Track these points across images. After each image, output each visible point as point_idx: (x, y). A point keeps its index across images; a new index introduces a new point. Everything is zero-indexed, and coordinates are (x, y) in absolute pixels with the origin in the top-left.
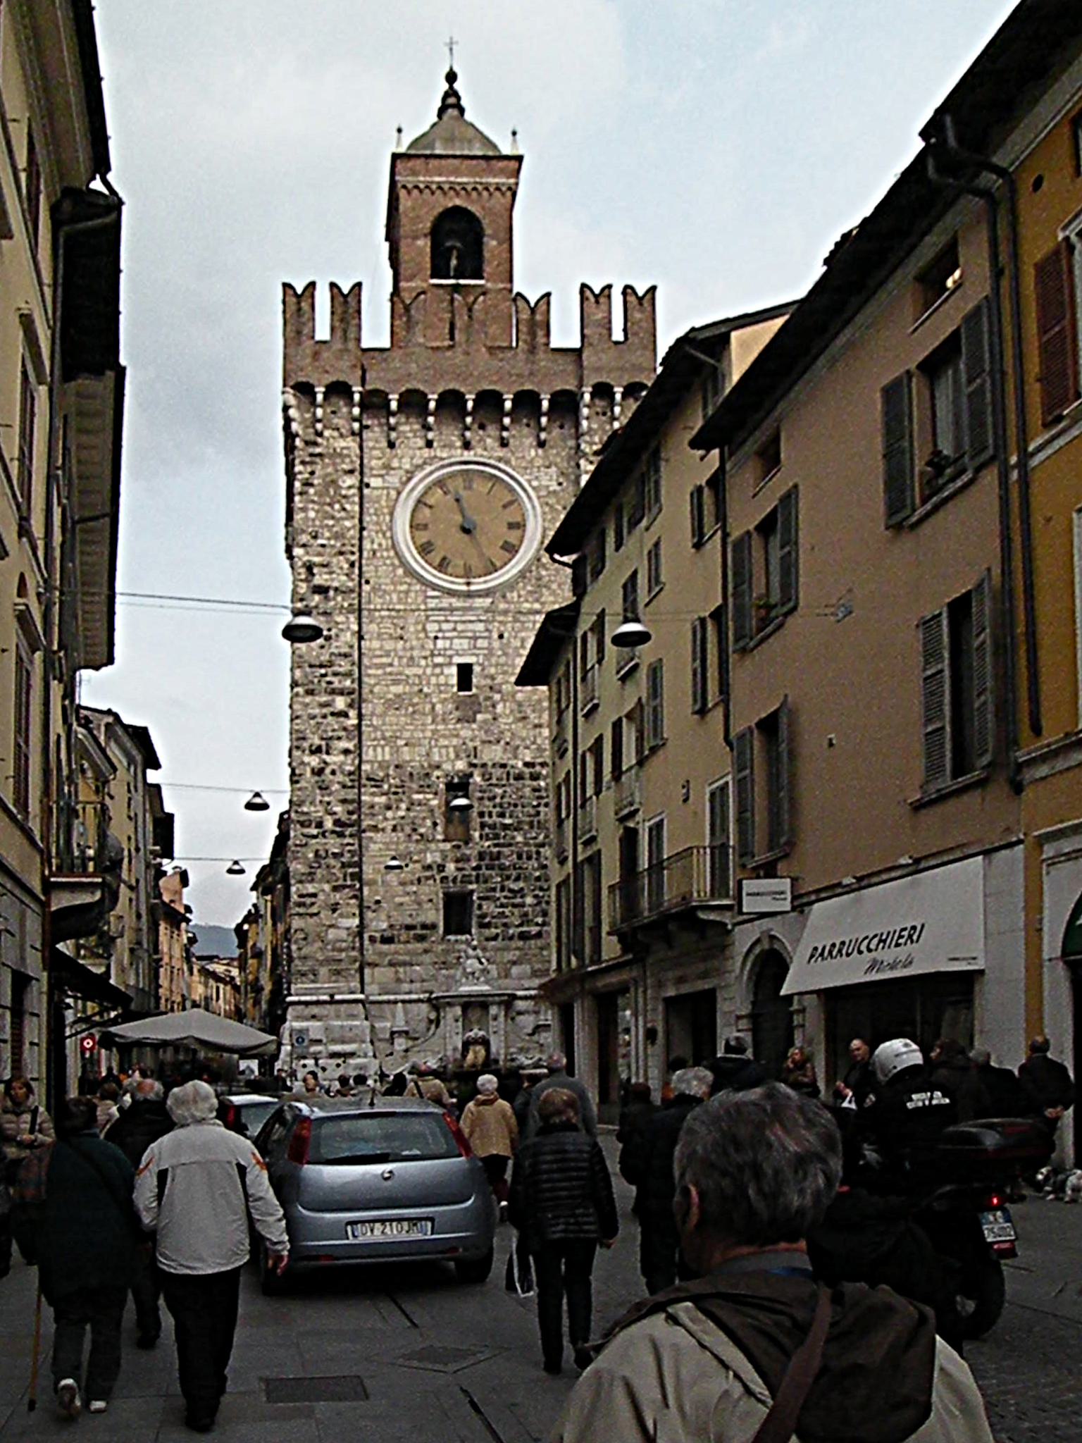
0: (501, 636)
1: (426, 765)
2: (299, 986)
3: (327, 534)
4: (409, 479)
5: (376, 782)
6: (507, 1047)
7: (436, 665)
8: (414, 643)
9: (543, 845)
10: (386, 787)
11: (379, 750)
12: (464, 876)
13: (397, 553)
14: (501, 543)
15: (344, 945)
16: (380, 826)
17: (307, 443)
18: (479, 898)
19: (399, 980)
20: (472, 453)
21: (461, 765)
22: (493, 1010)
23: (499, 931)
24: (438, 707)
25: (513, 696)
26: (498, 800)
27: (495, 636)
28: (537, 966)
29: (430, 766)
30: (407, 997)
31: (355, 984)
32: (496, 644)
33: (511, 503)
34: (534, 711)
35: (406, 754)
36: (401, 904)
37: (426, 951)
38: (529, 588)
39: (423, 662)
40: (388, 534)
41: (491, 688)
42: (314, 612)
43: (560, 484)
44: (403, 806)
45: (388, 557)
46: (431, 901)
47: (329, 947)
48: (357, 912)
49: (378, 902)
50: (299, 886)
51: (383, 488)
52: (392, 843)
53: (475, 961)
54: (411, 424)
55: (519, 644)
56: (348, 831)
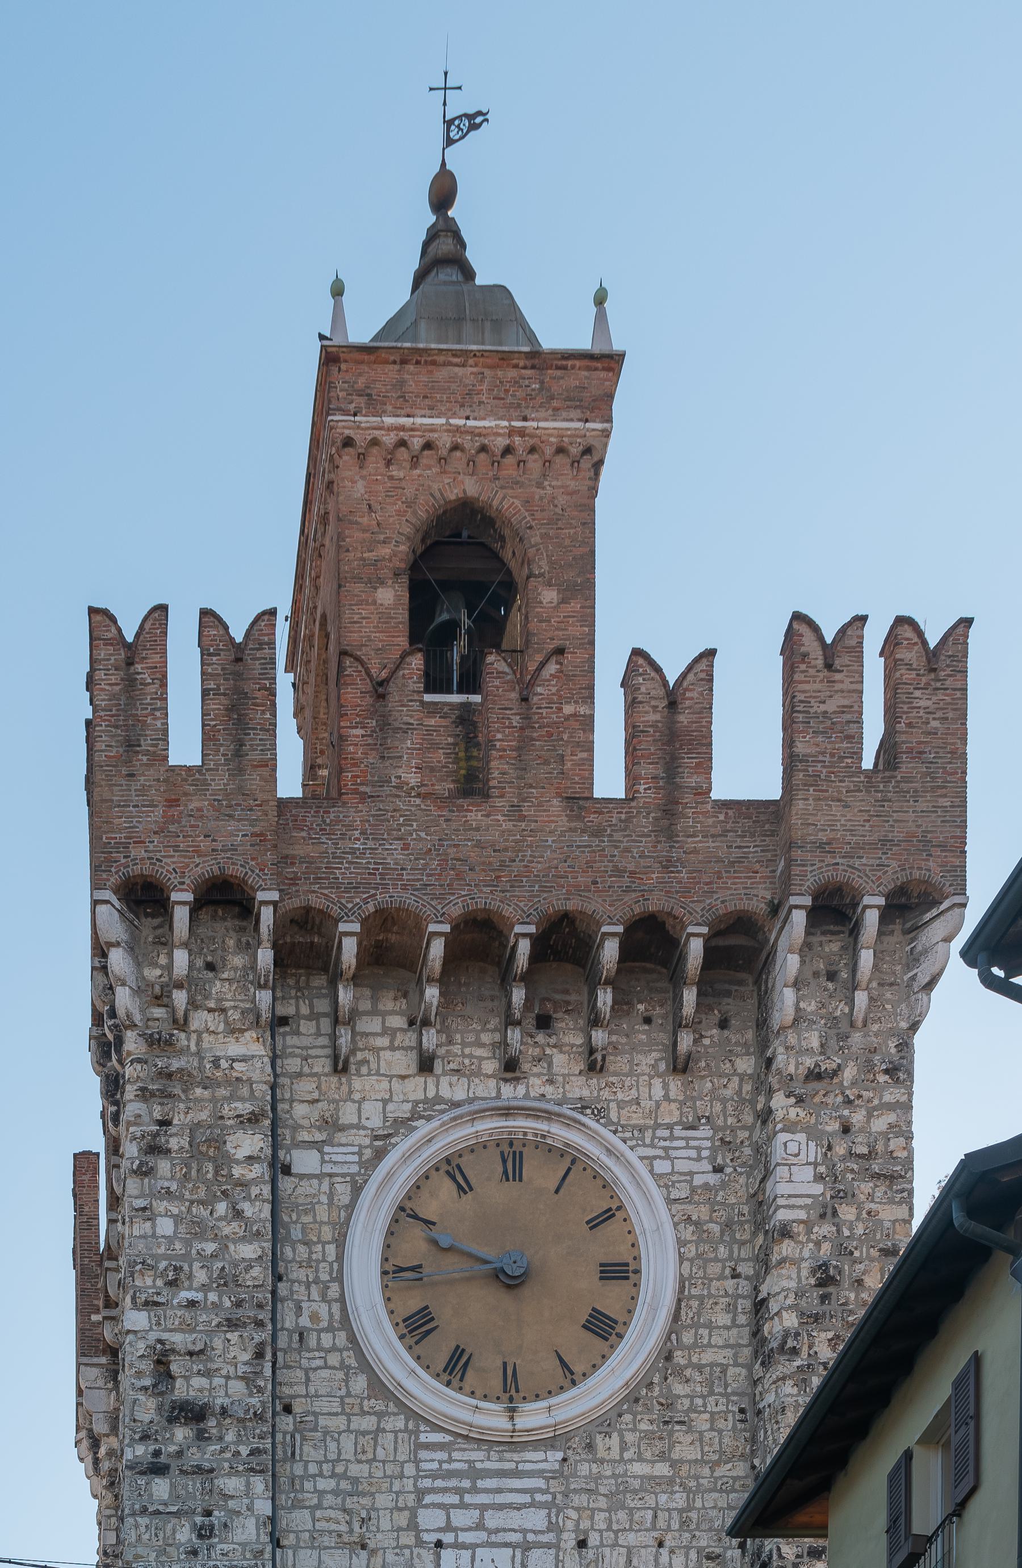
4: (380, 1155)
20: (521, 1090)
40: (334, 1291)
43: (718, 1170)
45: (334, 1349)
51: (320, 1177)
54: (384, 1014)
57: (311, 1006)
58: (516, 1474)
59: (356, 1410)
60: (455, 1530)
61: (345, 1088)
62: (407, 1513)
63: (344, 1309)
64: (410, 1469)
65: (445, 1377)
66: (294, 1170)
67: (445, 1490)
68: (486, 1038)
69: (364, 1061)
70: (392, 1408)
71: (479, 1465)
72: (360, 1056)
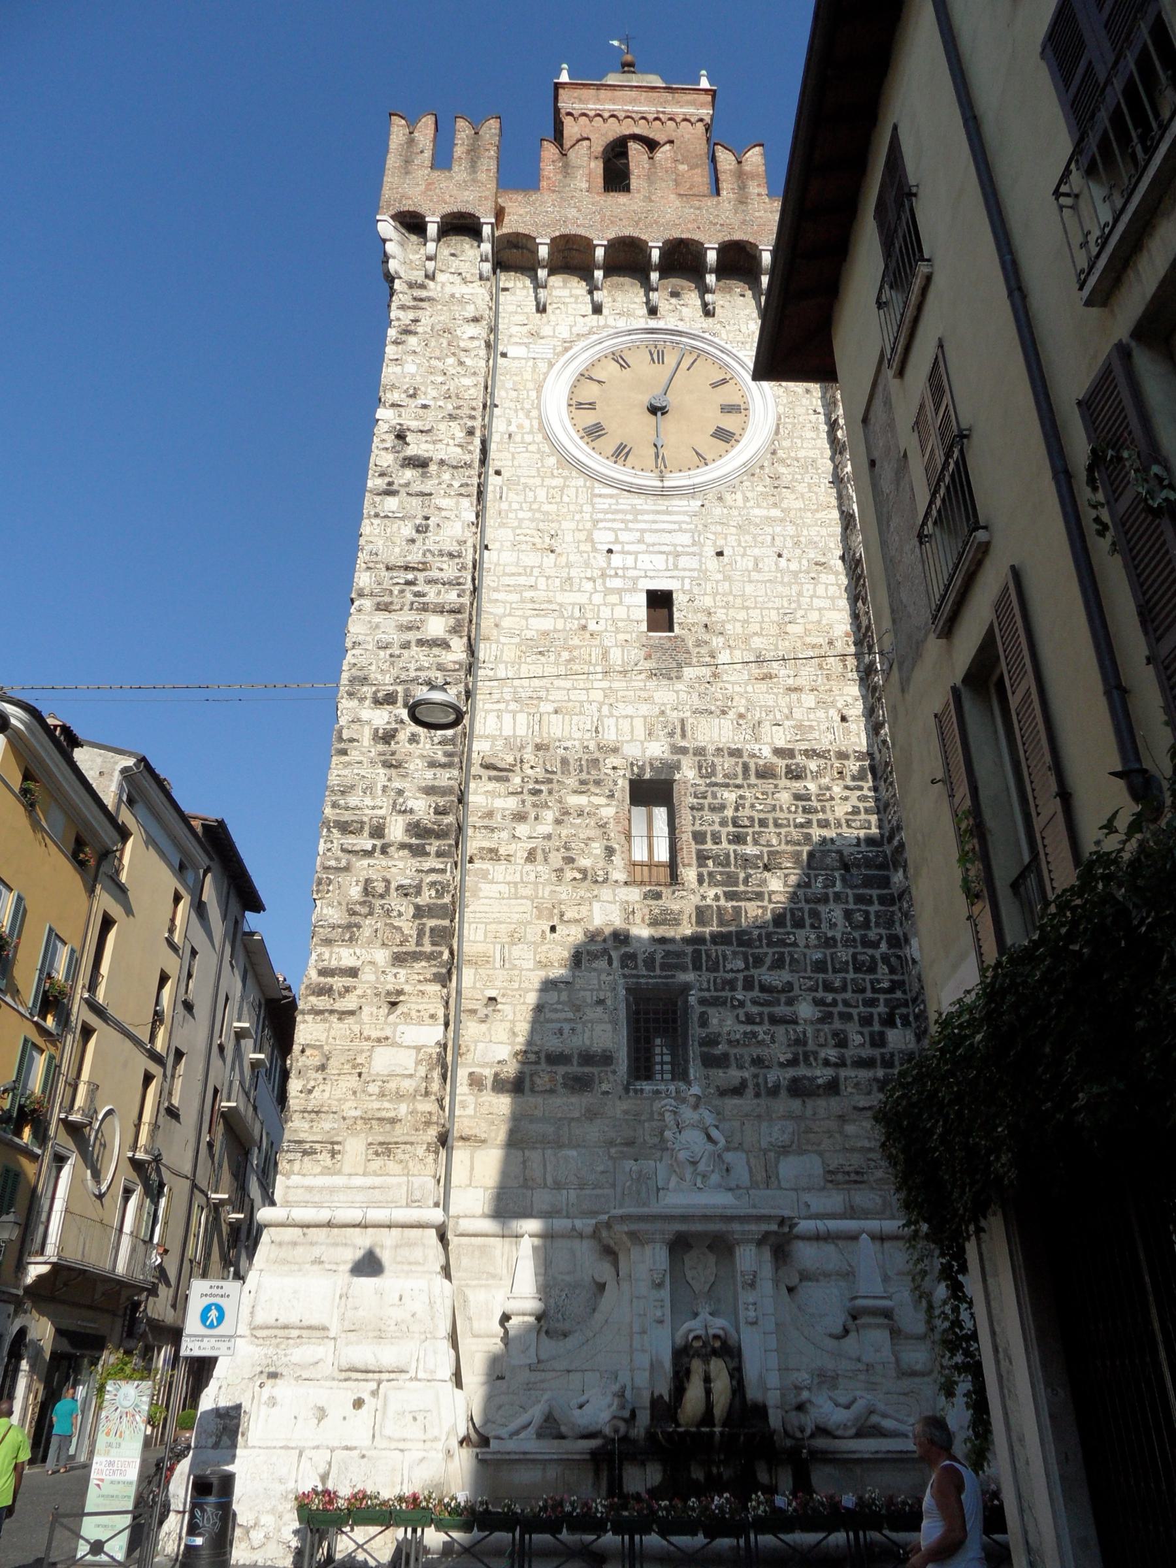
1: (592, 745)
3: (434, 393)
4: (566, 350)
6: (784, 1370)
7: (608, 591)
8: (572, 558)
9: (825, 899)
12: (668, 954)
13: (547, 438)
14: (712, 431)
15: (408, 1085)
17: (411, 285)
18: (702, 1002)
21: (658, 749)
22: (748, 1258)
24: (616, 656)
25: (746, 641)
26: (729, 813)
27: (710, 551)
28: (835, 1162)
29: (600, 748)
31: (425, 1183)
32: (712, 563)
38: (760, 489)
39: (588, 586)
41: (706, 626)
42: (403, 491)
46: (601, 1002)
48: (441, 1013)
50: (325, 951)
51: (528, 359)
52: (526, 884)
53: (700, 1137)
55: (751, 565)
56: (433, 846)
58: (667, 513)
59: (549, 474)
62: (585, 533)
63: (541, 423)
64: (587, 508)
65: (614, 459)
67: (614, 520)
68: (637, 300)
70: (574, 474)
71: (639, 507)
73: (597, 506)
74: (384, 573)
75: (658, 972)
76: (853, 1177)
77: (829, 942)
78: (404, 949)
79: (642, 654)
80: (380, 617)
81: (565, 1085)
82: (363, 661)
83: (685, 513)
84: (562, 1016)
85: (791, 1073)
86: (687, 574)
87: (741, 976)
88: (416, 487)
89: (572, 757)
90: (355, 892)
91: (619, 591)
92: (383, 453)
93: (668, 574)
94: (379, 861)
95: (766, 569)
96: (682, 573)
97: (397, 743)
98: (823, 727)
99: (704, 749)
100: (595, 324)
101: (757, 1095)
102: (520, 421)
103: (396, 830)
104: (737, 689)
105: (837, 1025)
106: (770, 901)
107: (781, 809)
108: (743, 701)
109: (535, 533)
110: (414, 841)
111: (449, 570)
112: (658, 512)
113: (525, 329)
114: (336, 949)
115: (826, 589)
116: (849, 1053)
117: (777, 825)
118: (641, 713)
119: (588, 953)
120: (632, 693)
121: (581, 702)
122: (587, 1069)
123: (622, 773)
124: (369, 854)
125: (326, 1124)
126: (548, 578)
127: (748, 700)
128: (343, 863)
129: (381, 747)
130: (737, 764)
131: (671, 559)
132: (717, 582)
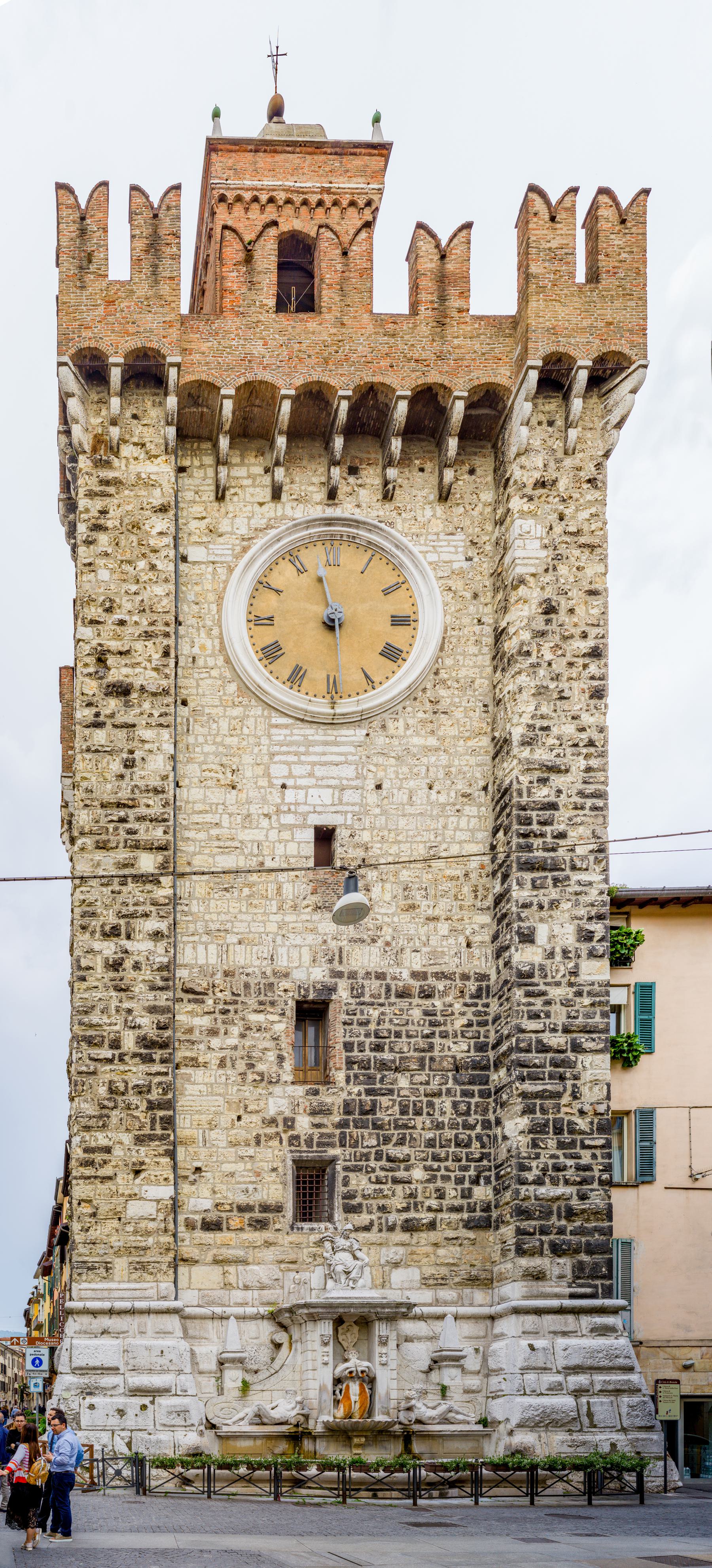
0: (379, 787)
1: (269, 972)
2: (85, 1285)
4: (245, 550)
5: (194, 994)
7: (282, 827)
9: (438, 1094)
10: (210, 1002)
11: (201, 948)
12: (322, 1135)
13: (228, 661)
14: (380, 648)
16: (201, 1060)
18: (346, 1169)
19: (227, 1286)
21: (319, 974)
23: (374, 1217)
26: (372, 1027)
28: (429, 1271)
29: (275, 973)
30: (240, 1311)
32: (372, 798)
33: (397, 586)
34: (426, 897)
35: (240, 957)
36: (232, 1175)
37: (268, 1244)
38: (421, 715)
39: (265, 823)
40: (215, 632)
44: (235, 1030)
46: (274, 1170)
47: (130, 1228)
49: (198, 1170)
54: (248, 466)
55: (405, 798)
57: (201, 460)
58: (336, 744)
59: (230, 704)
60: (294, 777)
61: (223, 510)
63: (222, 643)
64: (265, 741)
65: (289, 684)
66: (189, 559)
67: (289, 753)
69: (235, 494)
70: (253, 702)
71: (310, 738)
72: (232, 491)
73: (275, 738)
74: (100, 811)
75: (315, 1148)
76: (440, 1281)
77: (439, 1126)
78: (142, 1132)
79: (309, 889)
80: (99, 855)
81: (250, 1225)
82: (90, 898)
83: (351, 744)
84: (248, 1179)
85: (405, 1216)
86: (350, 808)
87: (373, 1150)
88: (120, 719)
89: (252, 981)
90: (103, 1091)
91: (291, 827)
92: (87, 680)
93: (333, 809)
94: (118, 1067)
95: (419, 802)
96: (346, 808)
97: (124, 970)
98: (452, 953)
99: (356, 973)
100: (272, 514)
101: (380, 1230)
102: (203, 641)
103: (129, 1042)
104: (386, 919)
105: (439, 1183)
106: (399, 1095)
107: (413, 1024)
108: (390, 930)
109: (219, 768)
110: (143, 1051)
111: (154, 806)
112: (326, 743)
113: (203, 524)
114: (93, 1133)
115: (469, 822)
116: (445, 1203)
117: (409, 1036)
118: (307, 942)
119: (265, 1135)
120: (300, 925)
121: (260, 933)
122: (264, 1215)
123: (291, 994)
124: (110, 1061)
125: (100, 1249)
126: (230, 815)
127: (394, 930)
128: (92, 1068)
129: (112, 974)
130: (381, 986)
131: (337, 793)
132: (376, 816)
